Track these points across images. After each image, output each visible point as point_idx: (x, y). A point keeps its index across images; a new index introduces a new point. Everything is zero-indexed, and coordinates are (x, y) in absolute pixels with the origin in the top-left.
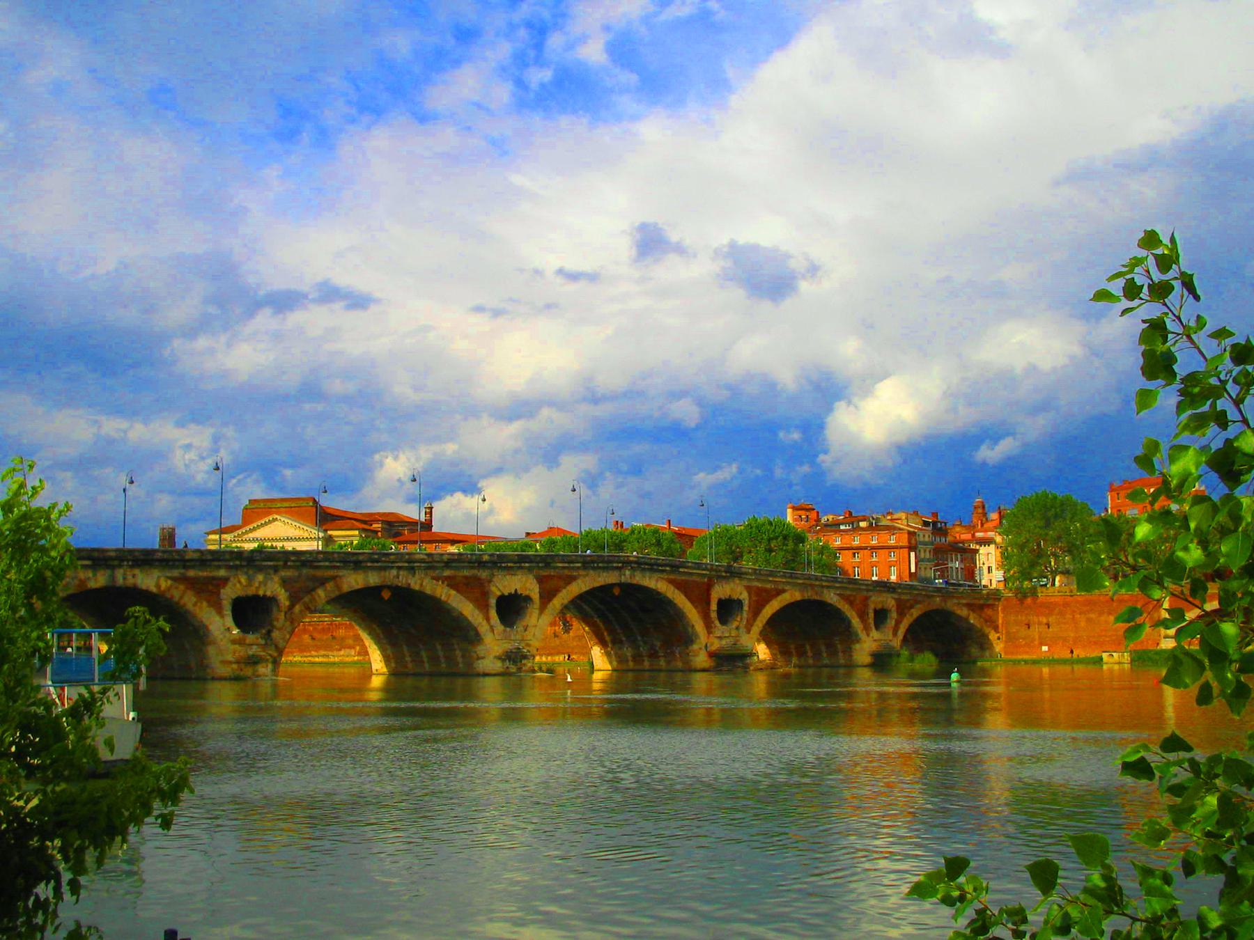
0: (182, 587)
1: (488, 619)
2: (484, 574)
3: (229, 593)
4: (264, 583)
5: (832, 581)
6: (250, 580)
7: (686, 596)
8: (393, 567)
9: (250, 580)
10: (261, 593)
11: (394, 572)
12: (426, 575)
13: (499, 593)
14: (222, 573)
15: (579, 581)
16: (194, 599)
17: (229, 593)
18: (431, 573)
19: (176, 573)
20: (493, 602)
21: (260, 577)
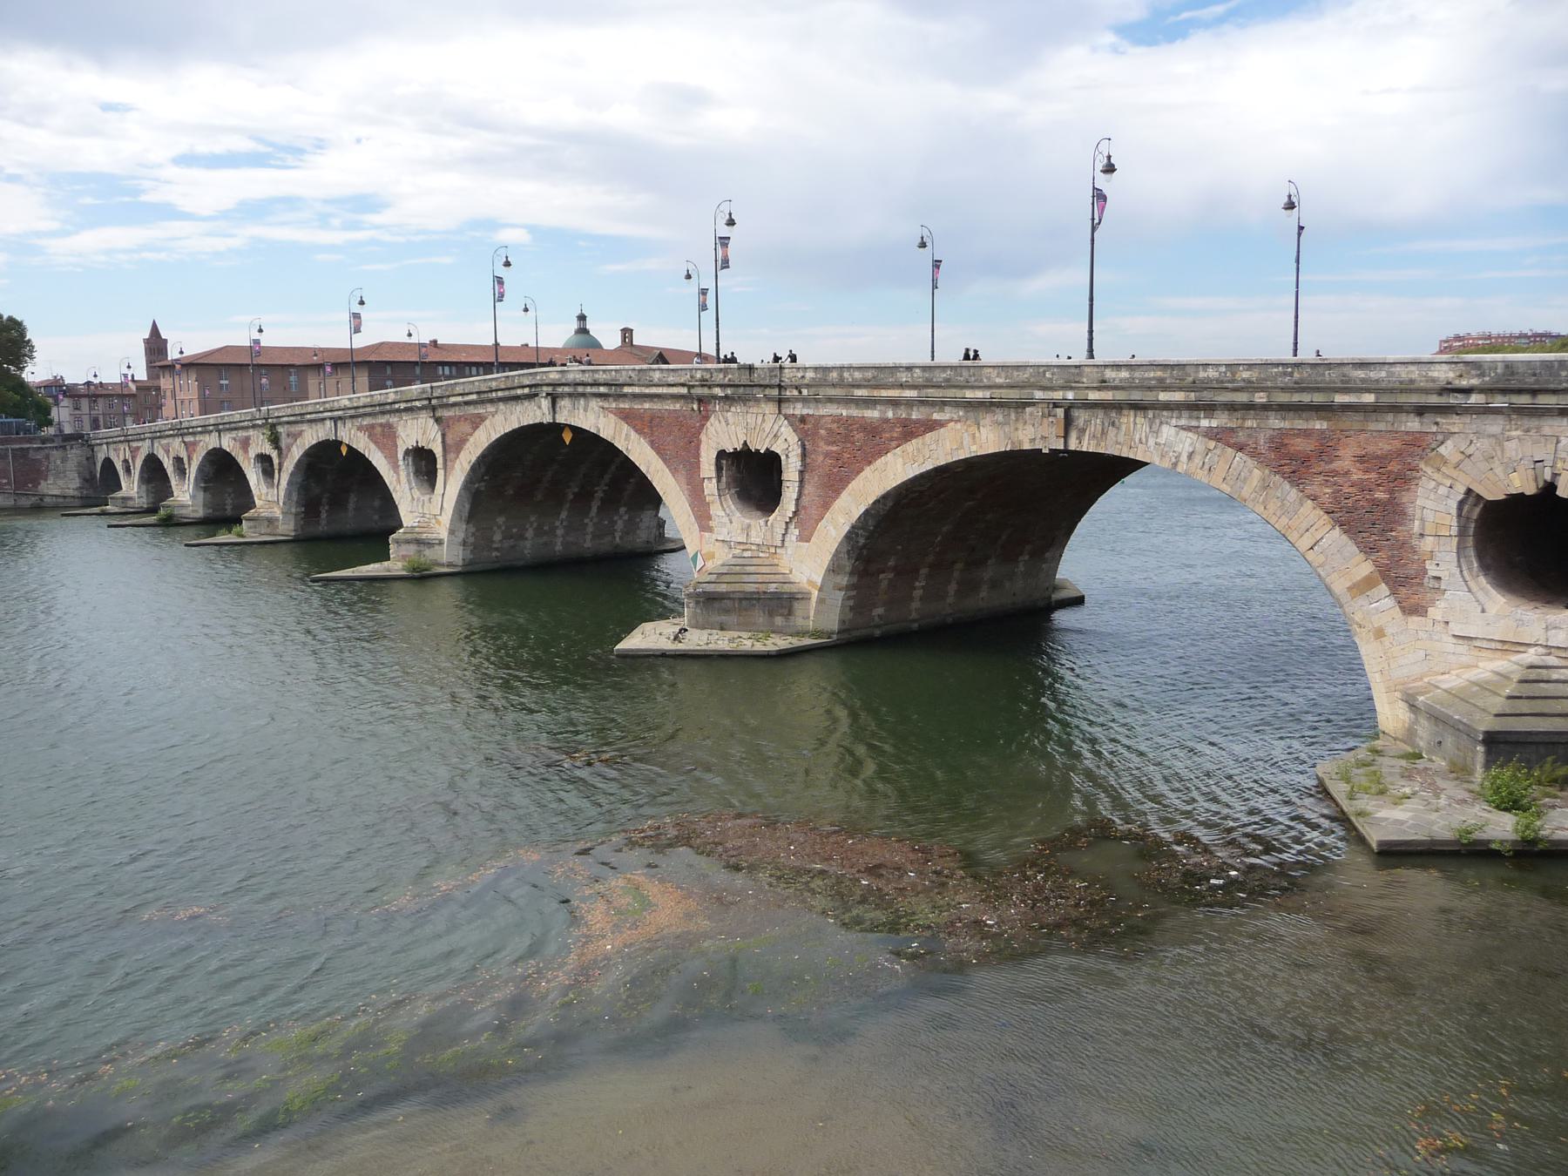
2: (393, 419)
3: (252, 453)
5: (1150, 389)
7: (652, 444)
8: (323, 419)
11: (328, 422)
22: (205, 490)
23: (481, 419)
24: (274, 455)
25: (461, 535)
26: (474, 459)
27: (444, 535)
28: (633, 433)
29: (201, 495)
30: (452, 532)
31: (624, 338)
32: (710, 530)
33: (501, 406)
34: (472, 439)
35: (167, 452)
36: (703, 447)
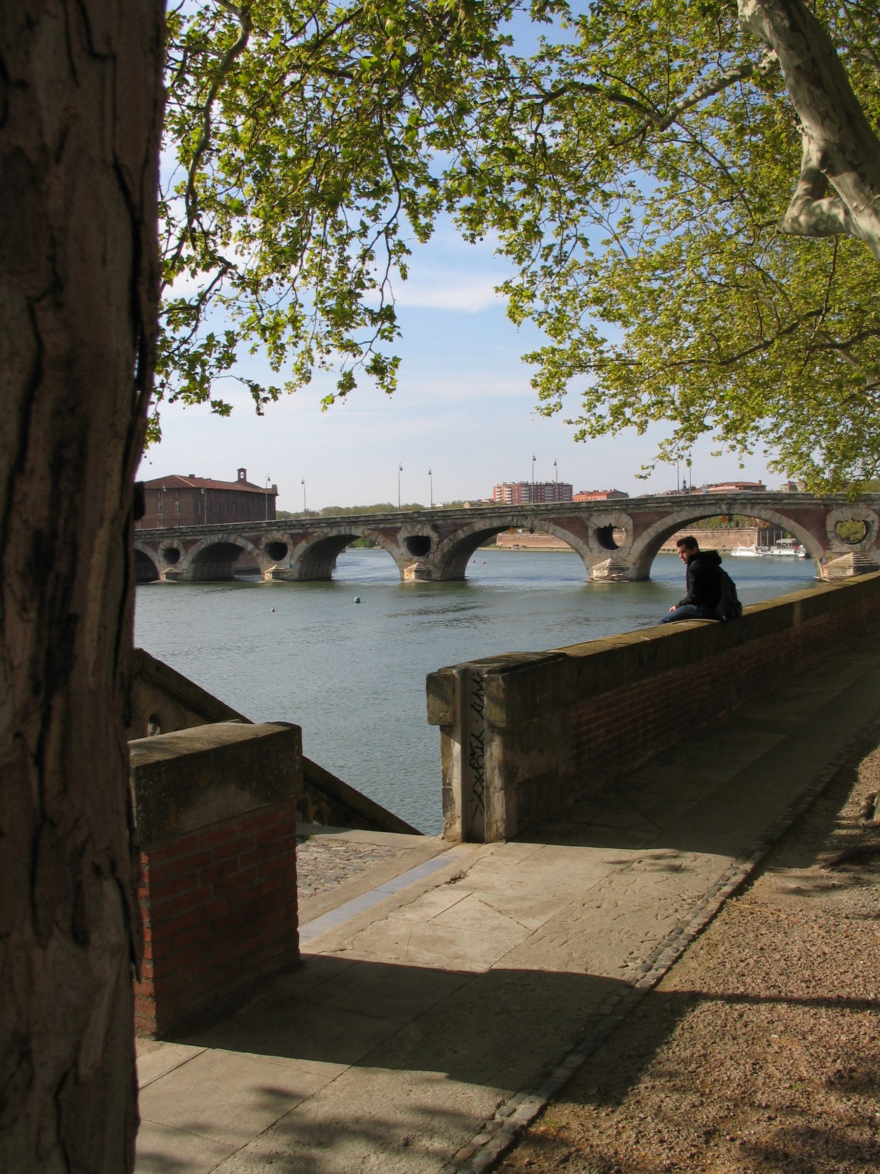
0: (376, 534)
1: (588, 544)
3: (402, 535)
4: (422, 529)
6: (413, 527)
7: (796, 521)
9: (413, 527)
10: (420, 534)
11: (510, 518)
12: (536, 518)
13: (595, 527)
14: (399, 525)
15: (674, 515)
16: (382, 540)
17: (402, 535)
18: (540, 517)
19: (373, 527)
20: (591, 532)
21: (419, 526)
22: (301, 562)
23: (668, 513)
24: (434, 536)
25: (637, 565)
26: (660, 530)
27: (630, 565)
28: (783, 517)
29: (299, 565)
30: (634, 564)
31: (239, 475)
32: (830, 549)
33: (686, 508)
34: (659, 523)
35: (256, 541)
36: (828, 522)
